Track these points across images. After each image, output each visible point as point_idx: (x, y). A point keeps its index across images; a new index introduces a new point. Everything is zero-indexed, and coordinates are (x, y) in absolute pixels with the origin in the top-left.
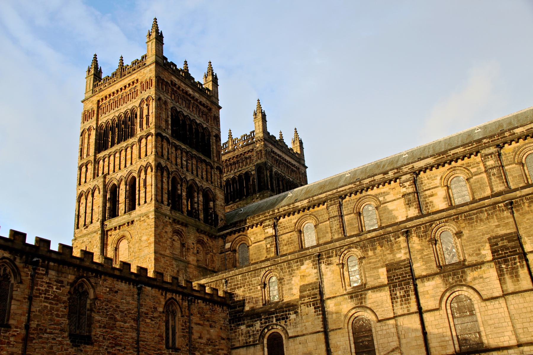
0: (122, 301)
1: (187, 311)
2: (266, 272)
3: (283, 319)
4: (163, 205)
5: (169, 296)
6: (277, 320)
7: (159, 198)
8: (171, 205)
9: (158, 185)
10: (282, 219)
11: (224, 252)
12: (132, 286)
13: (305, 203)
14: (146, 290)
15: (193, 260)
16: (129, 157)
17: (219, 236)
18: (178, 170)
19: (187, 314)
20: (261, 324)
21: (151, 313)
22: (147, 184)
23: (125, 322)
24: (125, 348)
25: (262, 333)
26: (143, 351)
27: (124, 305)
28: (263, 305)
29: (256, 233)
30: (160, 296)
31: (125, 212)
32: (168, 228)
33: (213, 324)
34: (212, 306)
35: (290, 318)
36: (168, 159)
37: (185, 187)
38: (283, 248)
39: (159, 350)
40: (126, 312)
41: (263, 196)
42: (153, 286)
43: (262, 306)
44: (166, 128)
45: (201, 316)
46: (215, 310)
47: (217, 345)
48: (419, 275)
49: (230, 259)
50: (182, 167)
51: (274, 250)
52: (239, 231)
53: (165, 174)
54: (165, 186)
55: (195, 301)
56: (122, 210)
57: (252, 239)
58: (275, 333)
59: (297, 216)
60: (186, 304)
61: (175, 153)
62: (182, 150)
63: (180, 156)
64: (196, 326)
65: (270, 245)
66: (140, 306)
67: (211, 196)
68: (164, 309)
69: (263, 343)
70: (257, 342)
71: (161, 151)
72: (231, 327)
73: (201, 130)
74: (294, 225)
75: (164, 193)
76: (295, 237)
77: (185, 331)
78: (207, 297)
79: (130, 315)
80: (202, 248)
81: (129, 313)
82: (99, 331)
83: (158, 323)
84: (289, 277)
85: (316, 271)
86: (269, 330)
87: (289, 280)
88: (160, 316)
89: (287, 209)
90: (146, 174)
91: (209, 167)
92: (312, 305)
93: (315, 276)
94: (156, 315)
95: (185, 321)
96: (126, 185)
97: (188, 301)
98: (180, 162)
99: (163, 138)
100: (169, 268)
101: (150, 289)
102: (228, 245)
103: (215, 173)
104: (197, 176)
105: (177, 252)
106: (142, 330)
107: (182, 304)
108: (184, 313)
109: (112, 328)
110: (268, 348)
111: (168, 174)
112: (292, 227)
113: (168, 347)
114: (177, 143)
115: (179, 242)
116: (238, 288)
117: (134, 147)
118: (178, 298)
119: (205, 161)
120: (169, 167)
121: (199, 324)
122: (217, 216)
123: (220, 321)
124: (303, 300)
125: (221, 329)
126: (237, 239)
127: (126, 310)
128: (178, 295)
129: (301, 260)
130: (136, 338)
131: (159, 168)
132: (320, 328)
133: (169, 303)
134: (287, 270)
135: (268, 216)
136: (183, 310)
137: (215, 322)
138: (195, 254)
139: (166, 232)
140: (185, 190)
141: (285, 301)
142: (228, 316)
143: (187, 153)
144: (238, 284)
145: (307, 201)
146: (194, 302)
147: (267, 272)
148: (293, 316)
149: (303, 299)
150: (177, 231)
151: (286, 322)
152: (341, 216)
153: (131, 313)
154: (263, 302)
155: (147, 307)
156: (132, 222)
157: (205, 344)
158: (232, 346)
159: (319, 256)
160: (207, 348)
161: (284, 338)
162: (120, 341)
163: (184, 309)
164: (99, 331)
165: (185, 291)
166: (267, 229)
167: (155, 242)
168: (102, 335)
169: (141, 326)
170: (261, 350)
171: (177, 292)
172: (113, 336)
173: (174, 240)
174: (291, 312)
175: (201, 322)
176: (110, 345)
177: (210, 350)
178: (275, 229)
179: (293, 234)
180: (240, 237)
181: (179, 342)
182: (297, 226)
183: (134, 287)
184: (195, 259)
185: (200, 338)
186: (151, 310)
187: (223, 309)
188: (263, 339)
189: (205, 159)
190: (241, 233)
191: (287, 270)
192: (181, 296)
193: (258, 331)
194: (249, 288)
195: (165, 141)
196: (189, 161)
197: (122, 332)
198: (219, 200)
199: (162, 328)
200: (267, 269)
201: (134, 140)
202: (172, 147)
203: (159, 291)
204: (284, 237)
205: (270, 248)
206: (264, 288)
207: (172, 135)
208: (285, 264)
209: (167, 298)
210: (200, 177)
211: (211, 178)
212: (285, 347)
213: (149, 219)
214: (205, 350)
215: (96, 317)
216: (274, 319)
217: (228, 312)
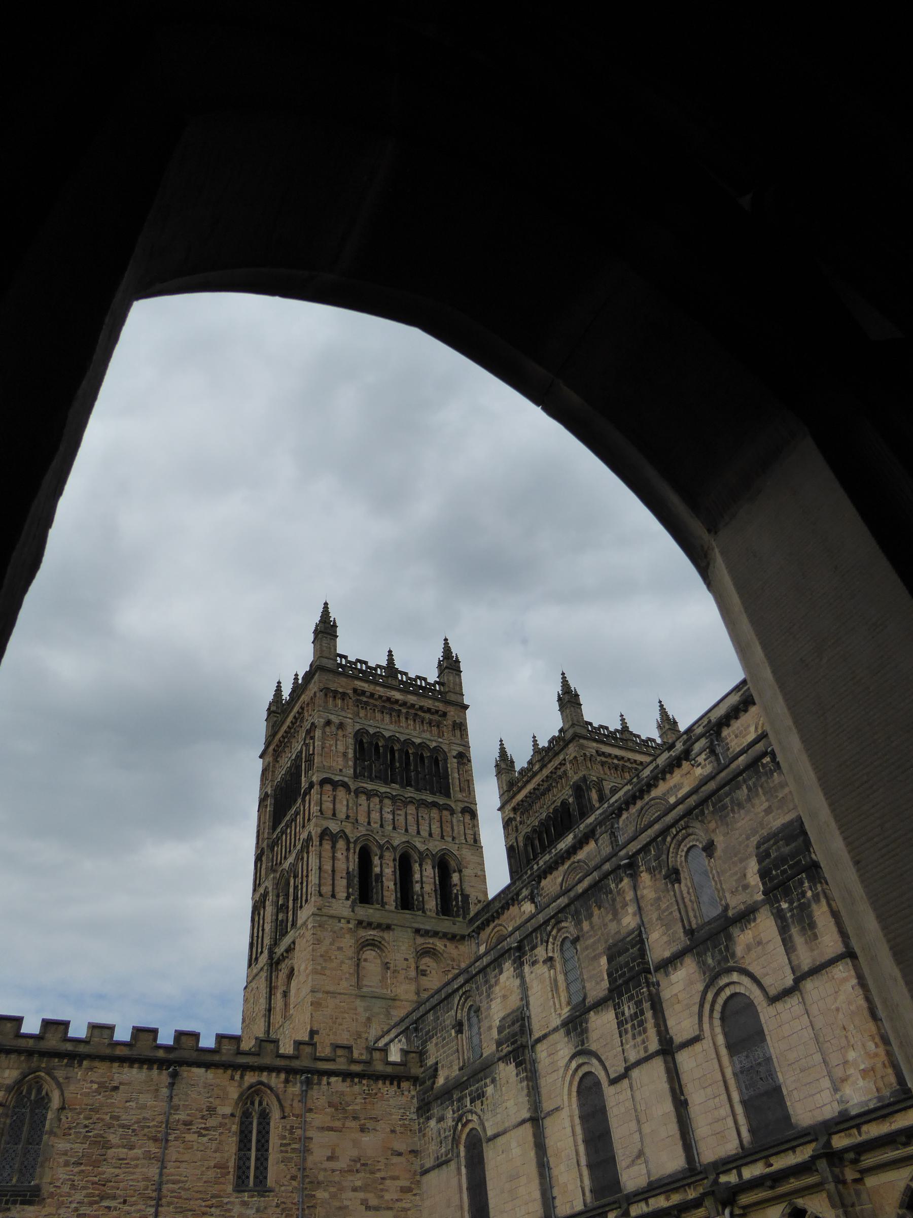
5: (250, 1078)
19: (297, 1112)
21: (200, 1120)
23: (132, 1148)
24: (125, 1202)
26: (169, 1204)
32: (345, 940)
40: (135, 1127)
45: (337, 1109)
46: (376, 1094)
47: (379, 1170)
48: (660, 958)
60: (295, 1089)
67: (453, 864)
73: (426, 754)
77: (289, 1148)
79: (146, 1130)
82: (62, 1174)
83: (216, 1139)
88: (221, 1125)
95: (292, 1127)
97: (301, 1083)
101: (203, 1070)
106: (173, 1159)
108: (287, 1110)
109: (96, 1164)
119: (434, 804)
121: (331, 1129)
123: (391, 1114)
125: (393, 1131)
127: (135, 1123)
130: (156, 1178)
133: (251, 1095)
136: (287, 1104)
137: (376, 1120)
139: (340, 949)
142: (415, 1100)
150: (371, 942)
153: (149, 1127)
155: (191, 1109)
157: (345, 1172)
160: (350, 1178)
162: (112, 1188)
164: (62, 1174)
165: (296, 1064)
168: (69, 1180)
171: (270, 1069)
172: (96, 1179)
175: (338, 1124)
176: (86, 1200)
177: (359, 1183)
185: (330, 1159)
186: (199, 1115)
187: (399, 1087)
189: (435, 800)
197: (120, 1168)
199: (226, 1149)
203: (225, 1072)
209: (246, 1085)
214: (345, 1184)
215: (60, 1145)
217: (413, 1093)
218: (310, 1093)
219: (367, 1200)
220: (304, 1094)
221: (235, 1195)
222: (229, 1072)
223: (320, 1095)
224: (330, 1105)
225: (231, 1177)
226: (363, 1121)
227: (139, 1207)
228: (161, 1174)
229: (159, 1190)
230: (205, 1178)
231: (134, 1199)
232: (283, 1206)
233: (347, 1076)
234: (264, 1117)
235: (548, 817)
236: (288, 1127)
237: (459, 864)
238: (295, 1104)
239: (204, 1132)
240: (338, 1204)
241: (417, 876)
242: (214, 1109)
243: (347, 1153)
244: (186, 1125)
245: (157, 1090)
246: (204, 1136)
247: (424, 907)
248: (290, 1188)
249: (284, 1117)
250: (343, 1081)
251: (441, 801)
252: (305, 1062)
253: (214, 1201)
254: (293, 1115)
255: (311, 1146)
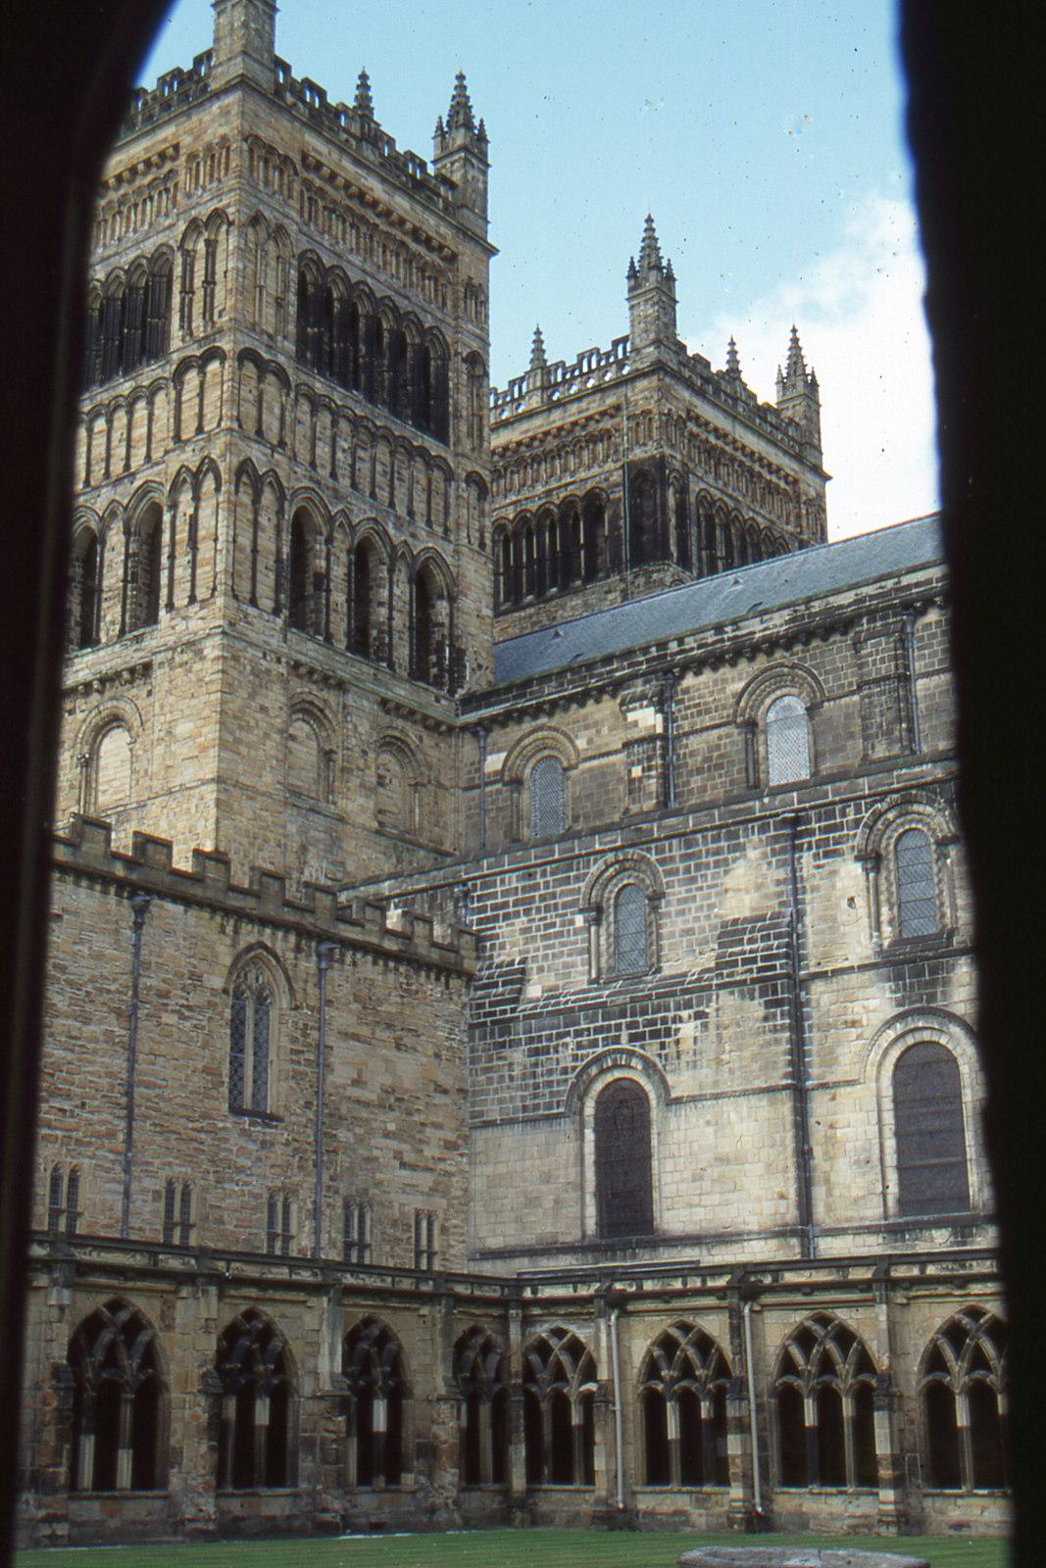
0: (76, 948)
1: (312, 990)
2: (608, 867)
3: (655, 1035)
4: (251, 610)
5: (249, 934)
6: (633, 1038)
7: (245, 587)
8: (285, 612)
9: (240, 539)
10: (689, 680)
11: (478, 787)
12: (112, 899)
13: (778, 623)
14: (163, 913)
15: (363, 809)
16: (140, 432)
17: (464, 728)
18: (318, 483)
19: (313, 1002)
20: (579, 1046)
21: (179, 992)
22: (201, 533)
23: (87, 1021)
25: (579, 1076)
26: (146, 1117)
27: (84, 963)
28: (591, 982)
29: (596, 724)
30: (215, 937)
31: (122, 632)
33: (408, 1040)
34: (406, 977)
35: (680, 1036)
36: (282, 444)
37: (345, 546)
38: (688, 783)
39: (205, 1116)
40: (89, 988)
41: (648, 582)
42: (188, 902)
43: (585, 986)
44: (277, 331)
45: (364, 1008)
46: (417, 992)
49: (499, 809)
50: (333, 475)
51: (653, 788)
52: (536, 711)
53: (268, 497)
54: (266, 541)
55: (343, 955)
56: (113, 623)
57: (581, 743)
58: (623, 1083)
59: (746, 669)
61: (308, 424)
62: (336, 414)
63: (328, 432)
64: (343, 1045)
65: (643, 770)
66: (138, 968)
68: (228, 981)
69: (581, 1111)
70: (562, 1110)
71: (253, 412)
72: (472, 1050)
74: (731, 701)
75: (260, 567)
76: (733, 743)
77: (302, 1057)
78: (391, 945)
79: (107, 997)
80: (398, 768)
81: (101, 990)
83: (203, 1028)
84: (687, 891)
85: (782, 874)
86: (602, 1072)
87: (685, 900)
88: (211, 1005)
89: (710, 640)
90: (196, 498)
91: (437, 474)
92: (757, 994)
93: (780, 894)
94: (195, 999)
95: (306, 1025)
96: (127, 533)
97: (319, 955)
98: (327, 457)
99: (263, 367)
100: (269, 834)
101: (181, 908)
102: (494, 762)
103: (458, 497)
104: (392, 504)
105: (306, 778)
106: (146, 1050)
107: (296, 965)
108: (300, 996)
110: (596, 1131)
111: (281, 498)
112: (724, 708)
113: (236, 1110)
114: (319, 386)
115: (314, 744)
116: (506, 917)
117: (160, 398)
118: (279, 949)
119: (422, 452)
120: (281, 473)
121: (356, 1038)
122: (458, 655)
123: (436, 1028)
124: (728, 976)
125: (437, 1056)
126: (526, 741)
127: (92, 980)
128: (280, 934)
129: (731, 832)
130: (124, 1075)
131: (244, 479)
132: (779, 1076)
133: (245, 960)
134: (681, 866)
135: (641, 663)
137: (416, 1033)
138: (370, 789)
139: (263, 709)
140: (344, 557)
141: (668, 970)
143: (356, 422)
144: (505, 905)
145: (786, 615)
146: (342, 961)
147: (611, 870)
148: (688, 1029)
149: (725, 972)
150: (307, 706)
151: (663, 1046)
152: (904, 679)
153: (109, 991)
154: (590, 973)
156: (147, 668)
158: (474, 1115)
159: (796, 821)
160: (382, 1118)
161: (653, 1103)
162: (65, 1081)
163: (301, 984)
166: (634, 709)
167: (223, 744)
169: (142, 1034)
170: (573, 1136)
171: (277, 925)
173: (293, 738)
174: (685, 1014)
175: (365, 1031)
177: (391, 1127)
178: (661, 711)
179: (728, 736)
180: (540, 734)
181: (278, 1093)
182: (742, 704)
183: (119, 904)
184: (371, 805)
185: (357, 1082)
186: (179, 983)
187: (447, 987)
188: (581, 1099)
190: (543, 720)
191: (681, 866)
192: (292, 938)
193: (565, 1071)
194: (545, 918)
195: (271, 378)
196: (361, 453)
197: (72, 1051)
198: (472, 595)
199: (218, 1045)
200: (610, 856)
201: (159, 373)
202: (296, 400)
203: (212, 918)
204: (695, 743)
205: (640, 779)
206: (598, 922)
207: (300, 358)
208: (675, 842)
209: (242, 945)
210: (401, 510)
211: (447, 514)
212: (654, 1131)
213: (203, 659)
216: (624, 1035)
217: (465, 999)
218: (330, 973)
219: (401, 1153)
220: (321, 972)
221: (232, 1119)
222: (218, 918)
223: (342, 979)
224: (357, 999)
227: (105, 1116)
229: (129, 1094)
231: (97, 1103)
232: (296, 1144)
233: (379, 954)
234: (261, 1000)
235: (544, 512)
236: (301, 1025)
237: (455, 580)
238: (310, 986)
240: (362, 1152)
241: (385, 593)
242: (199, 978)
243: (378, 1080)
244: (160, 996)
245: (117, 931)
246: (186, 1018)
247: (391, 656)
248: (303, 1120)
249: (296, 1008)
250: (375, 963)
251: (434, 448)
252: (322, 922)
254: (308, 1007)
255: (332, 1059)
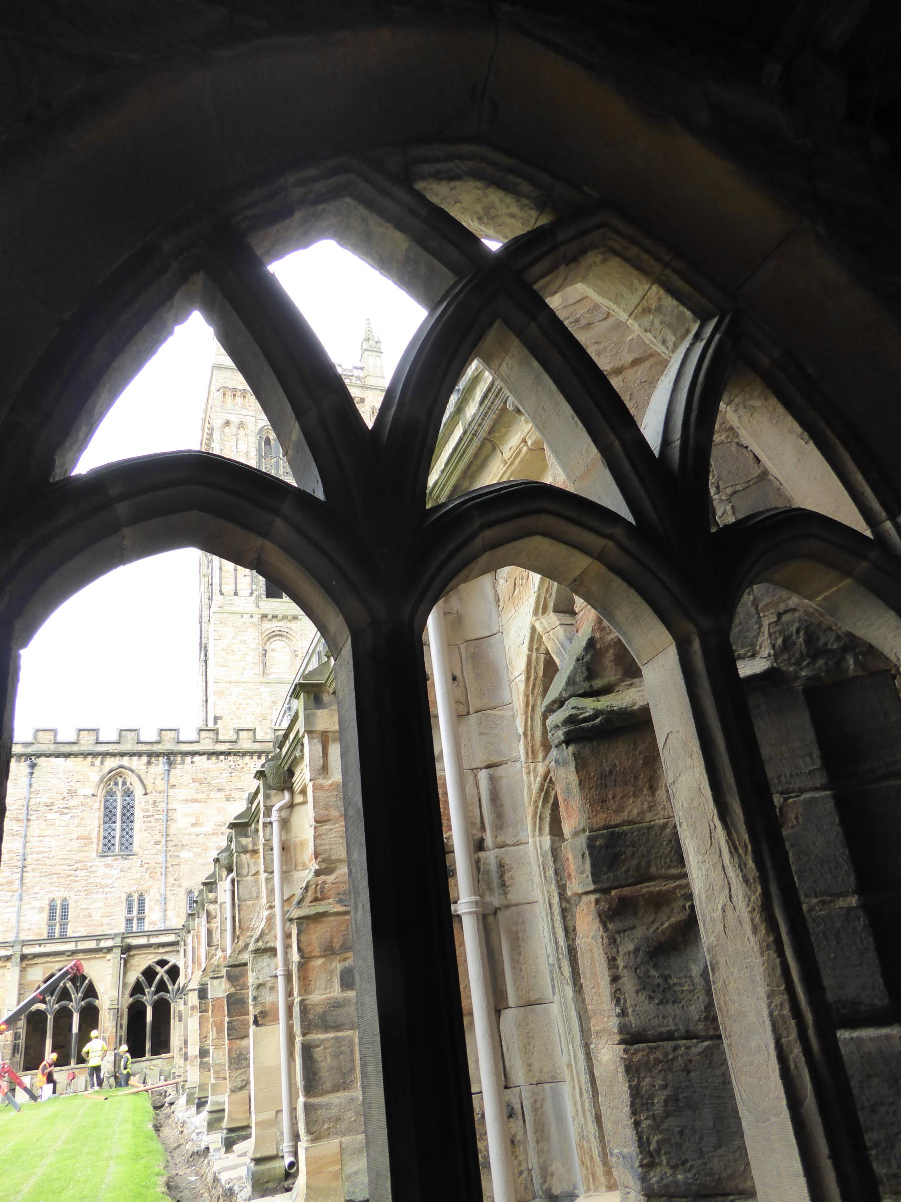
19: (158, 789)
21: (62, 801)
88: (82, 804)
95: (155, 802)
157: (209, 835)
171: (132, 754)
175: (201, 796)
185: (194, 825)
218: (173, 771)
225: (94, 846)
226: (228, 793)
228: (25, 847)
230: (68, 848)
232: (147, 866)
238: (158, 782)
239: (66, 811)
242: (75, 792)
248: (155, 852)
249: (146, 794)
252: (168, 745)
253: (78, 865)
254: (156, 791)
